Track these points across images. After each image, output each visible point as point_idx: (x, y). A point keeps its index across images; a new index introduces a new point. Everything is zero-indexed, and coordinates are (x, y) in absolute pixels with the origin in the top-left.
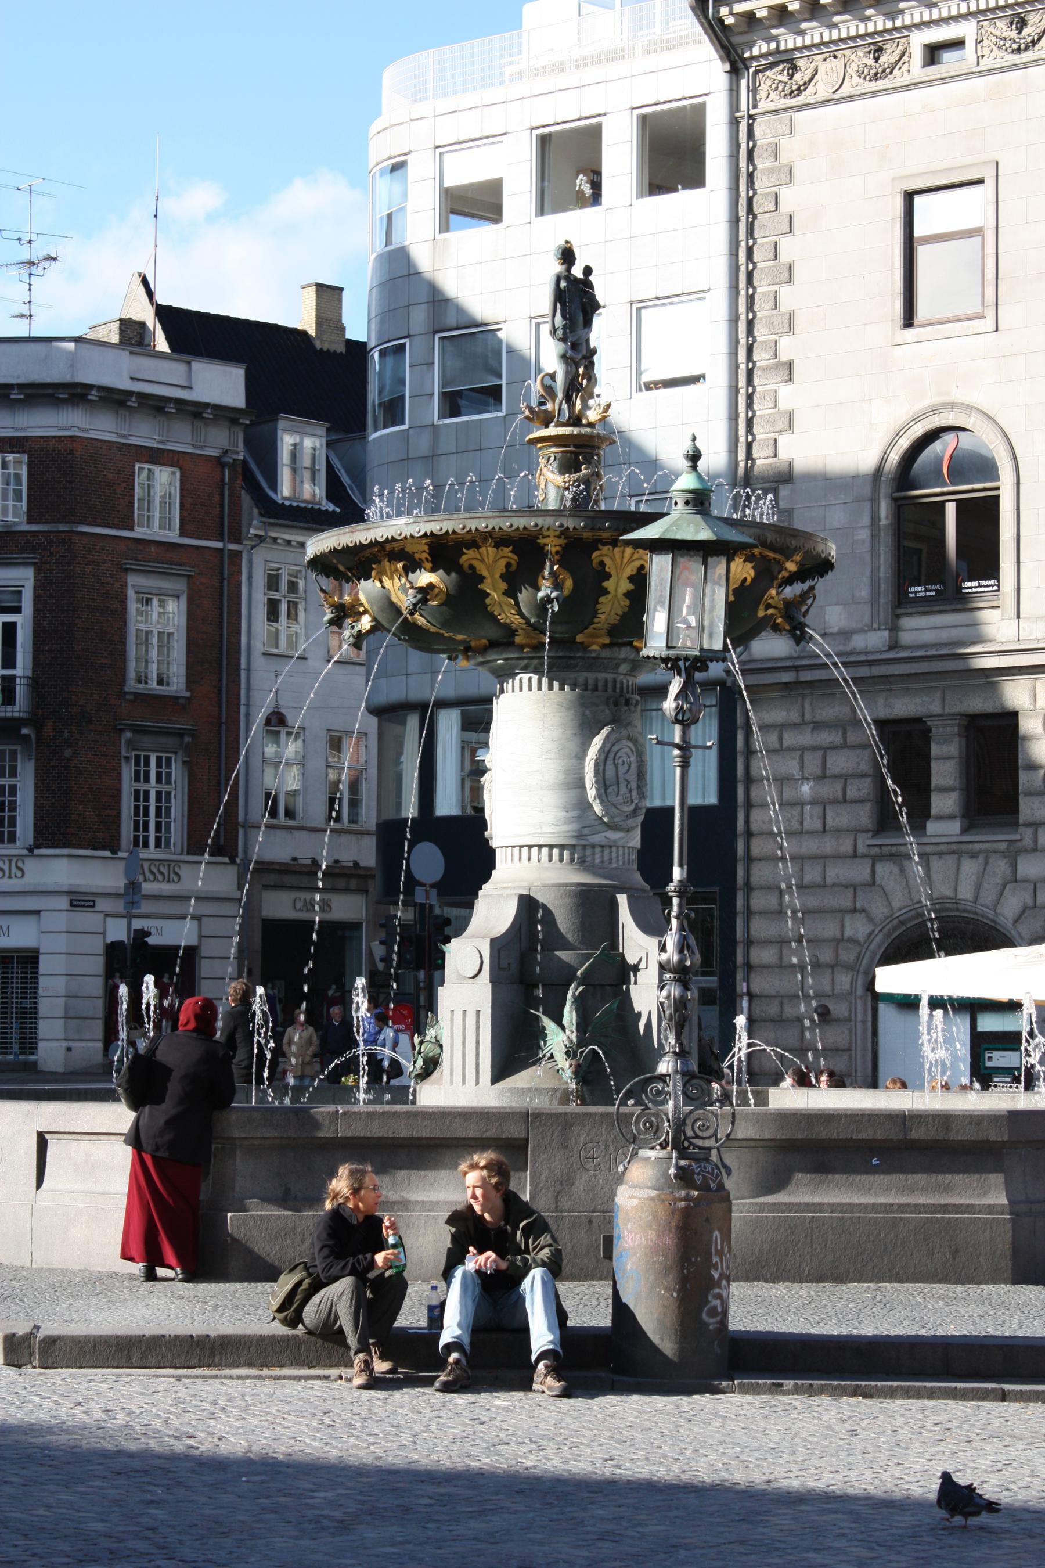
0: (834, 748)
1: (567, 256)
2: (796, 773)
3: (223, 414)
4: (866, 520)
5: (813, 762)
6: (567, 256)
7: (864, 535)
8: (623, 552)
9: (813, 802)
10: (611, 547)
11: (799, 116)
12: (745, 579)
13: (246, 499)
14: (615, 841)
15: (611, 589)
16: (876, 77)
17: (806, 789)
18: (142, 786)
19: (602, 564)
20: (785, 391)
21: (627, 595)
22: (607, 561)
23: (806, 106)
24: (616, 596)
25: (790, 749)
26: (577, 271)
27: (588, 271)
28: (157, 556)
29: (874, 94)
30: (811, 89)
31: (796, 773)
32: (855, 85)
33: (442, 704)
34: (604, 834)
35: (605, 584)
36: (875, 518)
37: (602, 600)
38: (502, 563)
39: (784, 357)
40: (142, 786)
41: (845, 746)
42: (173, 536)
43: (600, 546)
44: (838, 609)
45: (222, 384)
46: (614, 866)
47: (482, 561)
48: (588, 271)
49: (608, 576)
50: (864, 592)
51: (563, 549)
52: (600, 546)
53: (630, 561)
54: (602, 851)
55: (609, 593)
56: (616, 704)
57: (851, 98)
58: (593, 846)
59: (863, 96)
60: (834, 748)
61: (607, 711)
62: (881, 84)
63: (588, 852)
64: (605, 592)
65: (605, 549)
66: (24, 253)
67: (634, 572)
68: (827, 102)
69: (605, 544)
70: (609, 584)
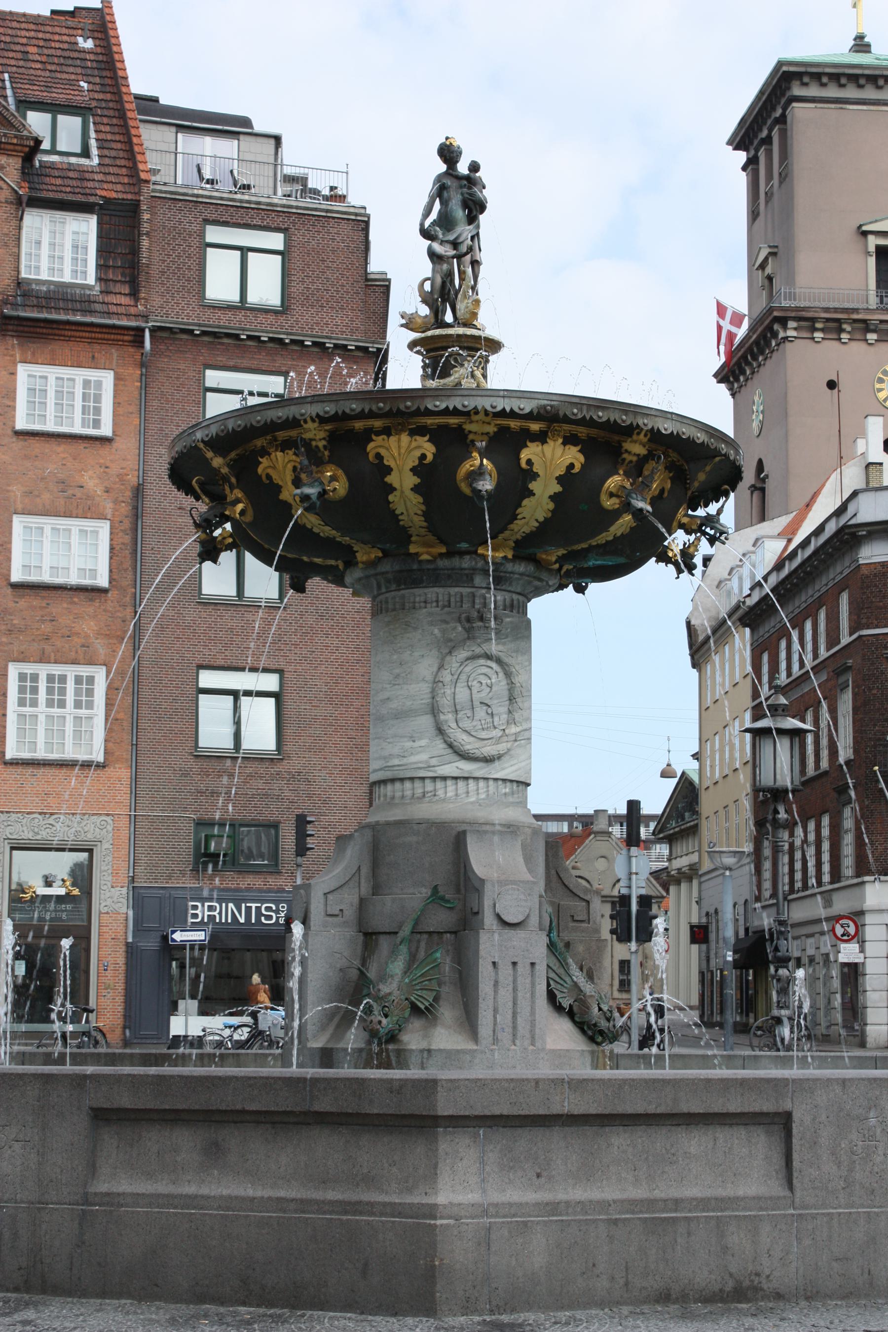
1: (448, 154)
6: (448, 154)
8: (399, 440)
10: (385, 437)
12: (571, 466)
15: (396, 485)
19: (379, 456)
21: (416, 489)
22: (383, 452)
24: (402, 492)
26: (463, 168)
27: (474, 167)
35: (388, 479)
37: (391, 498)
38: (290, 467)
43: (374, 437)
46: (473, 799)
47: (274, 468)
48: (474, 167)
49: (389, 470)
51: (329, 442)
52: (374, 437)
53: (409, 451)
55: (395, 489)
56: (468, 620)
64: (391, 489)
65: (379, 440)
67: (417, 463)
69: (378, 434)
70: (392, 479)
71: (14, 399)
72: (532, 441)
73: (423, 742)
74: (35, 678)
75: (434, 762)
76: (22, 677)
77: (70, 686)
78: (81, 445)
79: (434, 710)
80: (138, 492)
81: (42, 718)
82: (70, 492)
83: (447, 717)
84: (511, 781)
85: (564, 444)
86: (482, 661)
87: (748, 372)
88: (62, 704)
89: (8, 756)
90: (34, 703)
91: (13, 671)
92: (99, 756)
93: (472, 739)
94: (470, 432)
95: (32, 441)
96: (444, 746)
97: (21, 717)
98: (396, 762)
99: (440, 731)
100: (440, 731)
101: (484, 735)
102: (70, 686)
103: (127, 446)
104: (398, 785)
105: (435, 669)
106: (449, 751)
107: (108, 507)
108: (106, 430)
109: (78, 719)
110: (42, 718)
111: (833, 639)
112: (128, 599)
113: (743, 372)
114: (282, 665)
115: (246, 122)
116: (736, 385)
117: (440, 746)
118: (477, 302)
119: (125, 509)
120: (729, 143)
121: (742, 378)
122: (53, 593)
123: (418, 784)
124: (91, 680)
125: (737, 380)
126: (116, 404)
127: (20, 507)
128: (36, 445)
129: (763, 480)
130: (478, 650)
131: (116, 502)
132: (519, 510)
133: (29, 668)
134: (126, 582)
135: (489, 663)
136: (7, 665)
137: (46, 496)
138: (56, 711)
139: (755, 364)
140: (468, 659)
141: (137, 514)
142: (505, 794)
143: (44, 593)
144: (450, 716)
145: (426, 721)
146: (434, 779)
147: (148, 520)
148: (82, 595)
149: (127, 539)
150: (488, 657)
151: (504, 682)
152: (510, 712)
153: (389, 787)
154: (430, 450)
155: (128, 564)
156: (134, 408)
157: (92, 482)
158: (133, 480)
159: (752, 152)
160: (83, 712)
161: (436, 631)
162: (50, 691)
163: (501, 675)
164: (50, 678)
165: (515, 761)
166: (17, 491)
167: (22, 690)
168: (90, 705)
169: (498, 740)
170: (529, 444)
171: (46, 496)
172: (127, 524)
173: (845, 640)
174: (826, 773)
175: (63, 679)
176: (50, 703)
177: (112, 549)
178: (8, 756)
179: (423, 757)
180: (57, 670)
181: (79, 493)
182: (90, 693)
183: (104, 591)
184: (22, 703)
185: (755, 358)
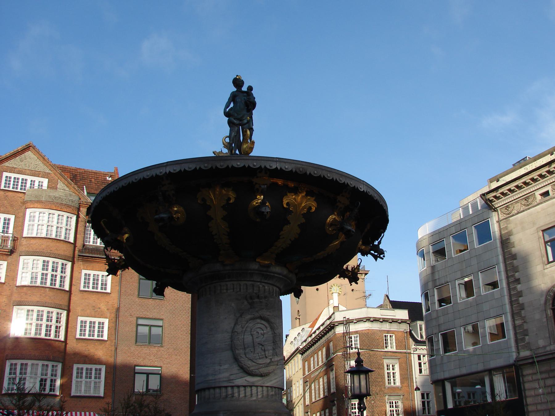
0: (546, 378)
2: (537, 387)
3: (403, 321)
4: (545, 316)
5: (542, 383)
7: (545, 320)
9: (543, 394)
11: (511, 218)
13: (411, 340)
14: (253, 382)
16: (528, 205)
17: (540, 391)
18: (392, 409)
20: (519, 287)
23: (513, 215)
25: (535, 380)
28: (392, 355)
29: (529, 209)
30: (513, 212)
31: (537, 387)
32: (524, 208)
33: (446, 379)
34: (245, 378)
36: (547, 315)
39: (517, 277)
40: (392, 409)
41: (550, 377)
42: (394, 349)
44: (542, 340)
45: (403, 314)
46: (254, 398)
50: (548, 335)
54: (245, 390)
55: (213, 219)
56: (251, 298)
57: (523, 211)
58: (238, 387)
59: (526, 210)
60: (546, 378)
61: (246, 303)
62: (530, 206)
63: (236, 390)
66: (363, 295)
68: (518, 213)
71: (80, 281)
72: (290, 192)
73: (226, 366)
74: (82, 369)
75: (232, 377)
76: (78, 369)
77: (93, 372)
79: (232, 348)
80: (118, 310)
81: (84, 382)
82: (96, 310)
83: (240, 352)
84: (275, 388)
85: (307, 195)
86: (259, 321)
88: (90, 378)
89: (72, 394)
90: (81, 377)
91: (75, 366)
92: (102, 394)
93: (255, 364)
94: (256, 183)
95: (85, 293)
96: (238, 368)
97: (77, 382)
98: (211, 378)
99: (236, 359)
100: (236, 359)
101: (260, 361)
102: (93, 372)
103: (115, 295)
104: (212, 391)
105: (232, 325)
106: (242, 371)
107: (108, 315)
108: (109, 290)
109: (95, 383)
110: (84, 382)
112: (113, 344)
114: (162, 364)
117: (235, 369)
118: (253, 143)
119: (113, 315)
122: (89, 342)
123: (223, 390)
124: (100, 370)
126: (112, 283)
127: (80, 314)
130: (257, 315)
131: (111, 313)
132: (282, 233)
133: (80, 366)
134: (113, 338)
135: (263, 322)
136: (73, 365)
137: (88, 311)
138: (88, 380)
140: (251, 319)
141: (117, 316)
142: (272, 395)
143: (86, 341)
144: (241, 351)
145: (229, 354)
146: (232, 387)
147: (121, 319)
148: (99, 342)
149: (114, 325)
150: (262, 318)
151: (270, 333)
152: (274, 349)
153: (207, 392)
154: (232, 195)
155: (113, 333)
156: (117, 284)
157: (103, 307)
158: (116, 306)
160: (97, 380)
161: (233, 305)
162: (87, 373)
163: (269, 328)
164: (87, 369)
165: (277, 377)
166: (79, 309)
167: (78, 373)
168: (100, 378)
169: (268, 365)
170: (289, 194)
171: (88, 311)
172: (114, 320)
175: (91, 369)
176: (86, 377)
177: (109, 328)
178: (72, 394)
179: (226, 375)
180: (89, 366)
181: (99, 310)
182: (100, 374)
183: (106, 341)
184: (77, 377)
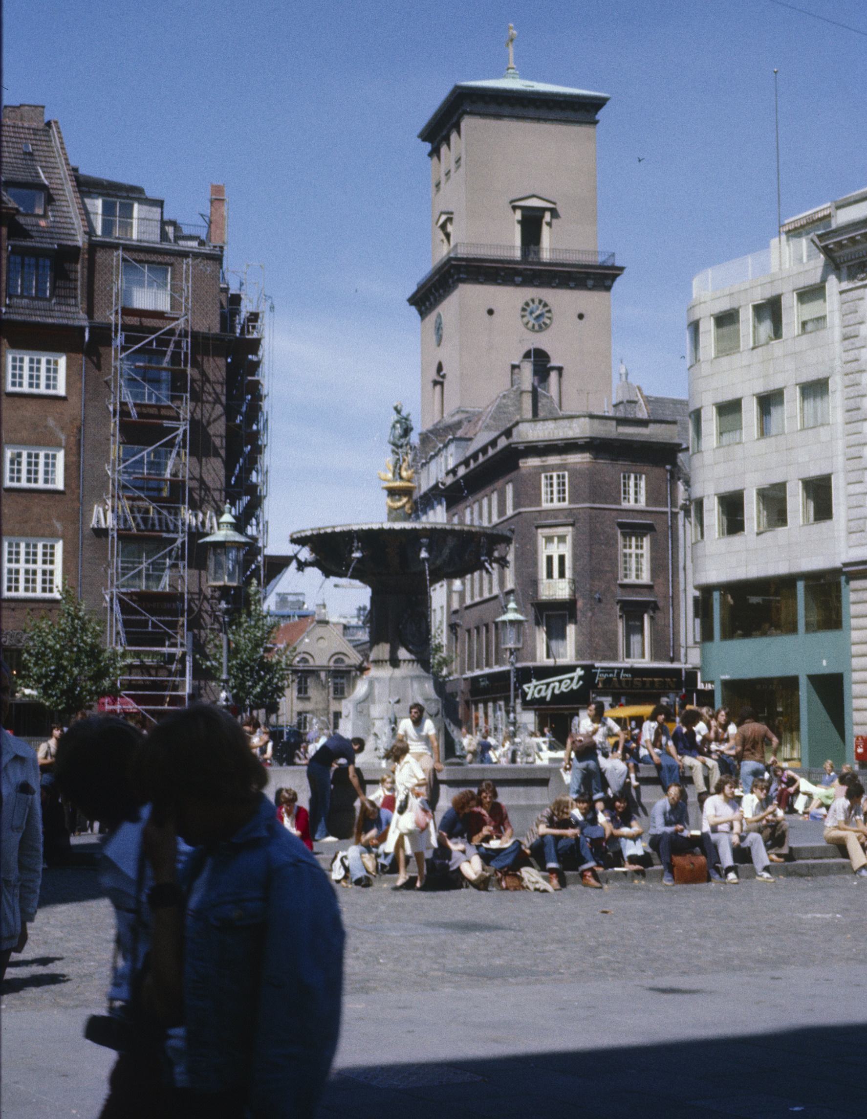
78: (46, 401)
81: (22, 572)
87: (432, 300)
108: (61, 391)
110: (22, 572)
111: (502, 511)
113: (429, 300)
115: (140, 190)
116: (423, 308)
120: (419, 137)
121: (427, 304)
125: (425, 305)
128: (18, 402)
129: (443, 377)
139: (437, 295)
159: (436, 144)
173: (510, 512)
174: (496, 597)
185: (437, 290)
